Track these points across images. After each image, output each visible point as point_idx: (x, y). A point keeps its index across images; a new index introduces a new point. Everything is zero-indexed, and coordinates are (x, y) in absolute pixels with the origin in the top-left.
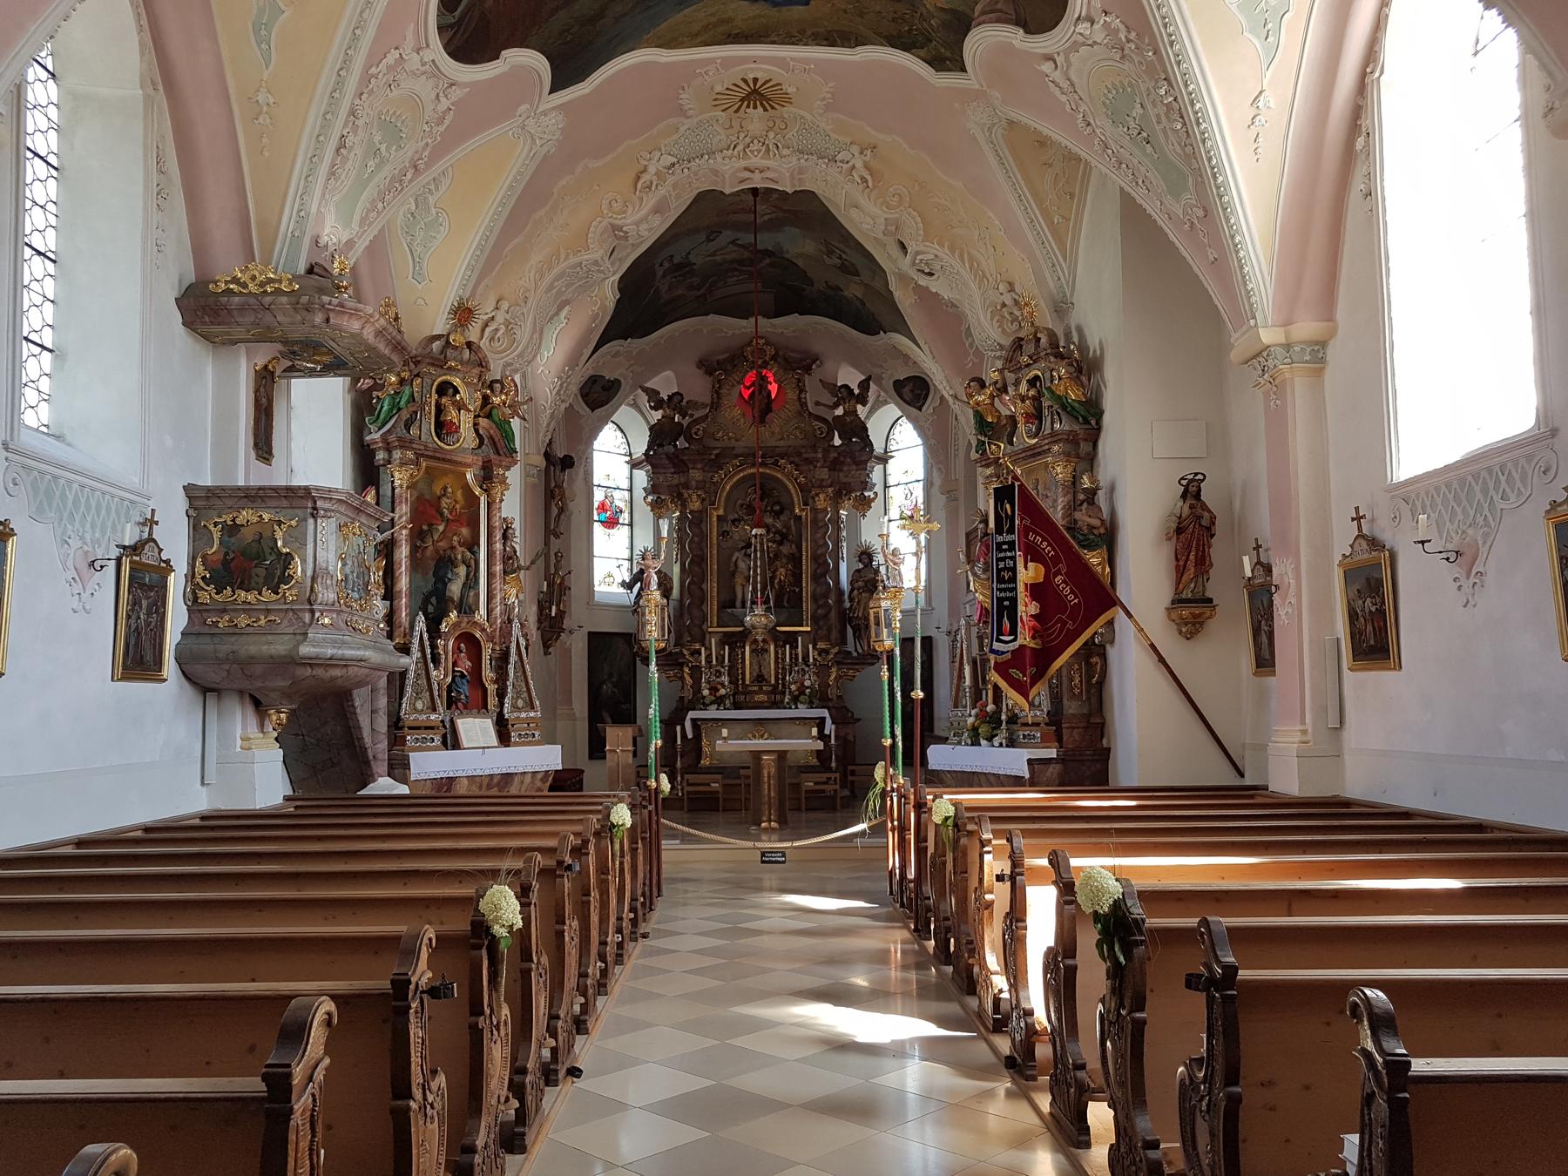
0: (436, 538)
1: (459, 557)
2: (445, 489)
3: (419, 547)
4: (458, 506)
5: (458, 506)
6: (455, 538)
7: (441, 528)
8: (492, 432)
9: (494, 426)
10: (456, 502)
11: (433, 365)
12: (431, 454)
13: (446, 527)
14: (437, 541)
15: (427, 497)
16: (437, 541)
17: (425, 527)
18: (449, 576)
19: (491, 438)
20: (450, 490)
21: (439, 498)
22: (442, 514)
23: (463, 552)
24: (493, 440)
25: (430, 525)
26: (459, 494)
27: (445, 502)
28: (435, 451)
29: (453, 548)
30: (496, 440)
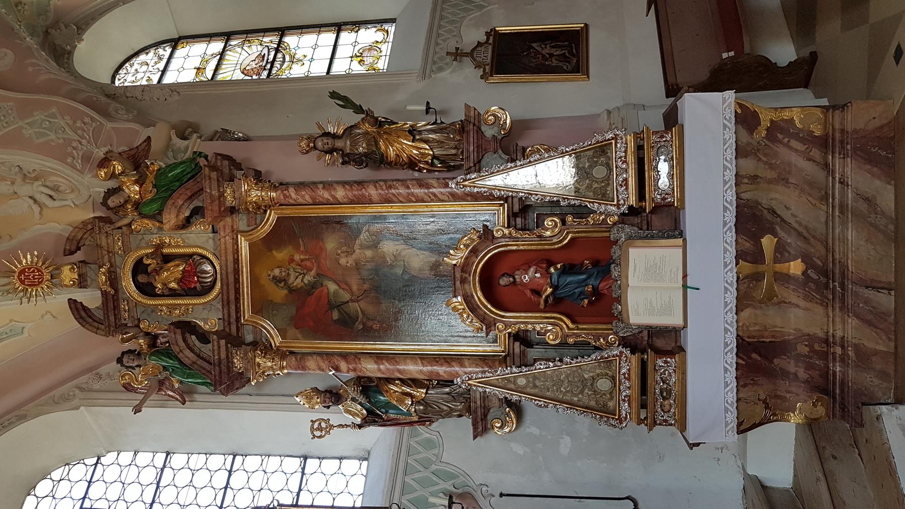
0: (346, 296)
1: (369, 253)
2: (277, 280)
3: (364, 324)
4: (297, 257)
5: (297, 257)
6: (343, 261)
7: (332, 287)
8: (180, 202)
9: (170, 202)
10: (291, 260)
11: (116, 307)
12: (233, 307)
13: (331, 279)
14: (352, 294)
15: (293, 311)
16: (352, 294)
17: (335, 315)
18: (399, 271)
19: (191, 198)
20: (277, 272)
21: (291, 290)
22: (313, 286)
23: (362, 247)
24: (190, 197)
25: (332, 306)
26: (281, 255)
27: (296, 282)
28: (226, 304)
29: (358, 266)
30: (189, 194)
